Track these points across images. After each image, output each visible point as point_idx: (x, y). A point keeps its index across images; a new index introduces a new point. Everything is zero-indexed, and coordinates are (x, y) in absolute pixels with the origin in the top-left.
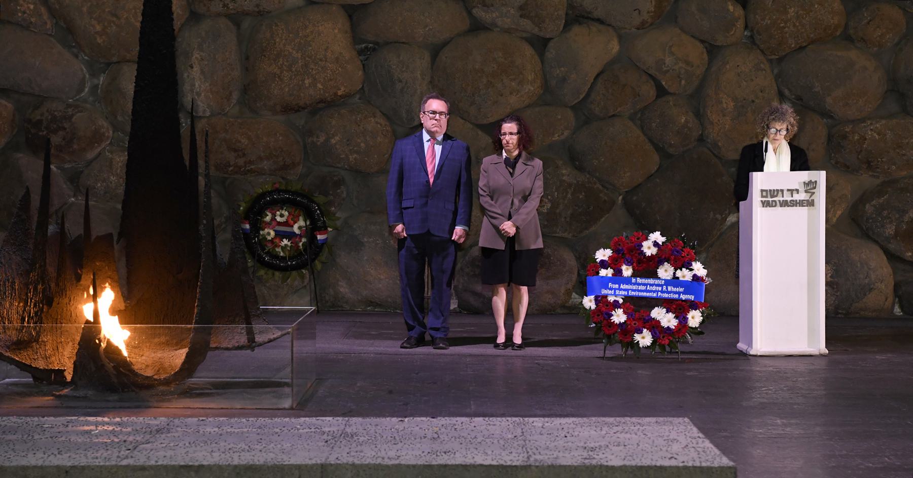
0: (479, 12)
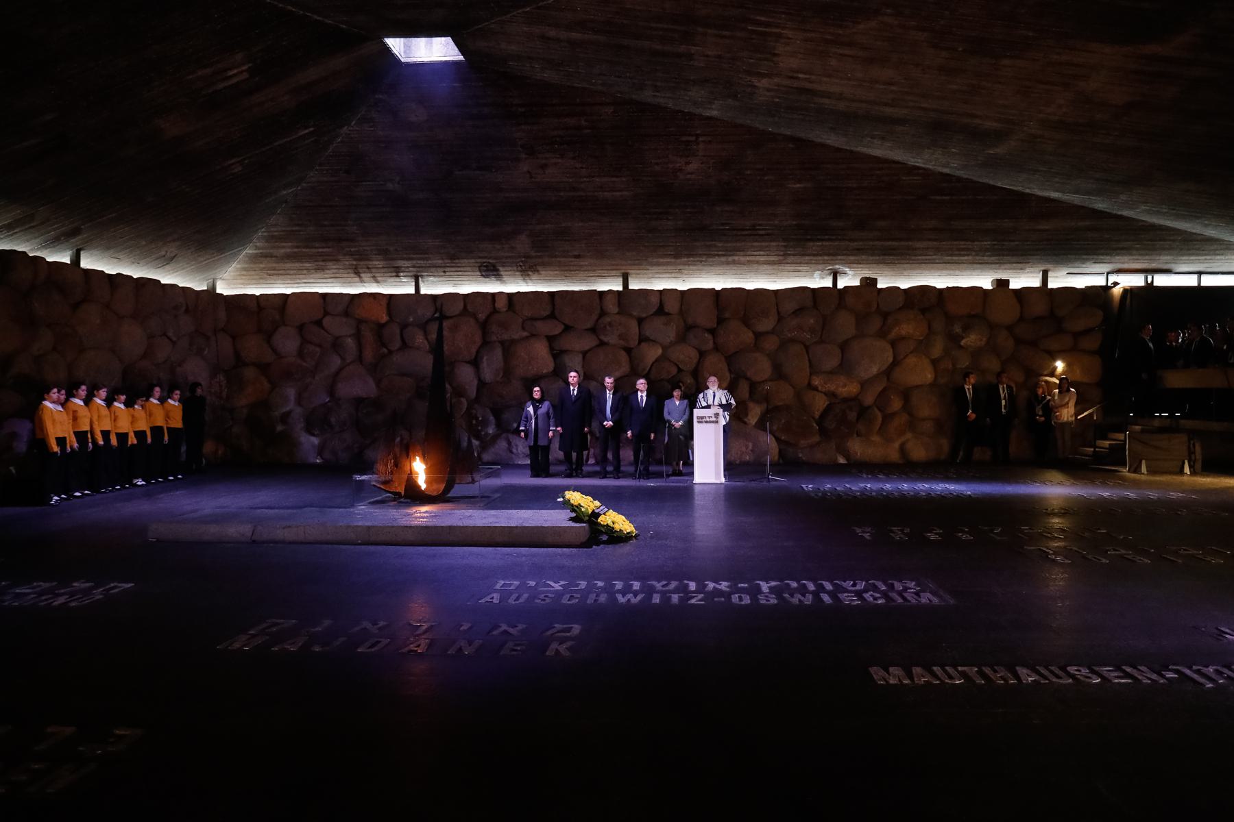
0: (602, 338)
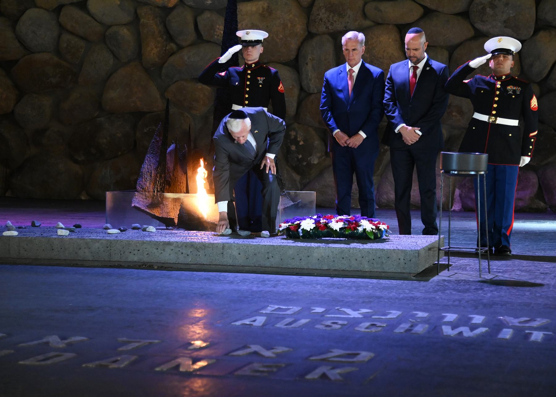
0: (479, 26)
